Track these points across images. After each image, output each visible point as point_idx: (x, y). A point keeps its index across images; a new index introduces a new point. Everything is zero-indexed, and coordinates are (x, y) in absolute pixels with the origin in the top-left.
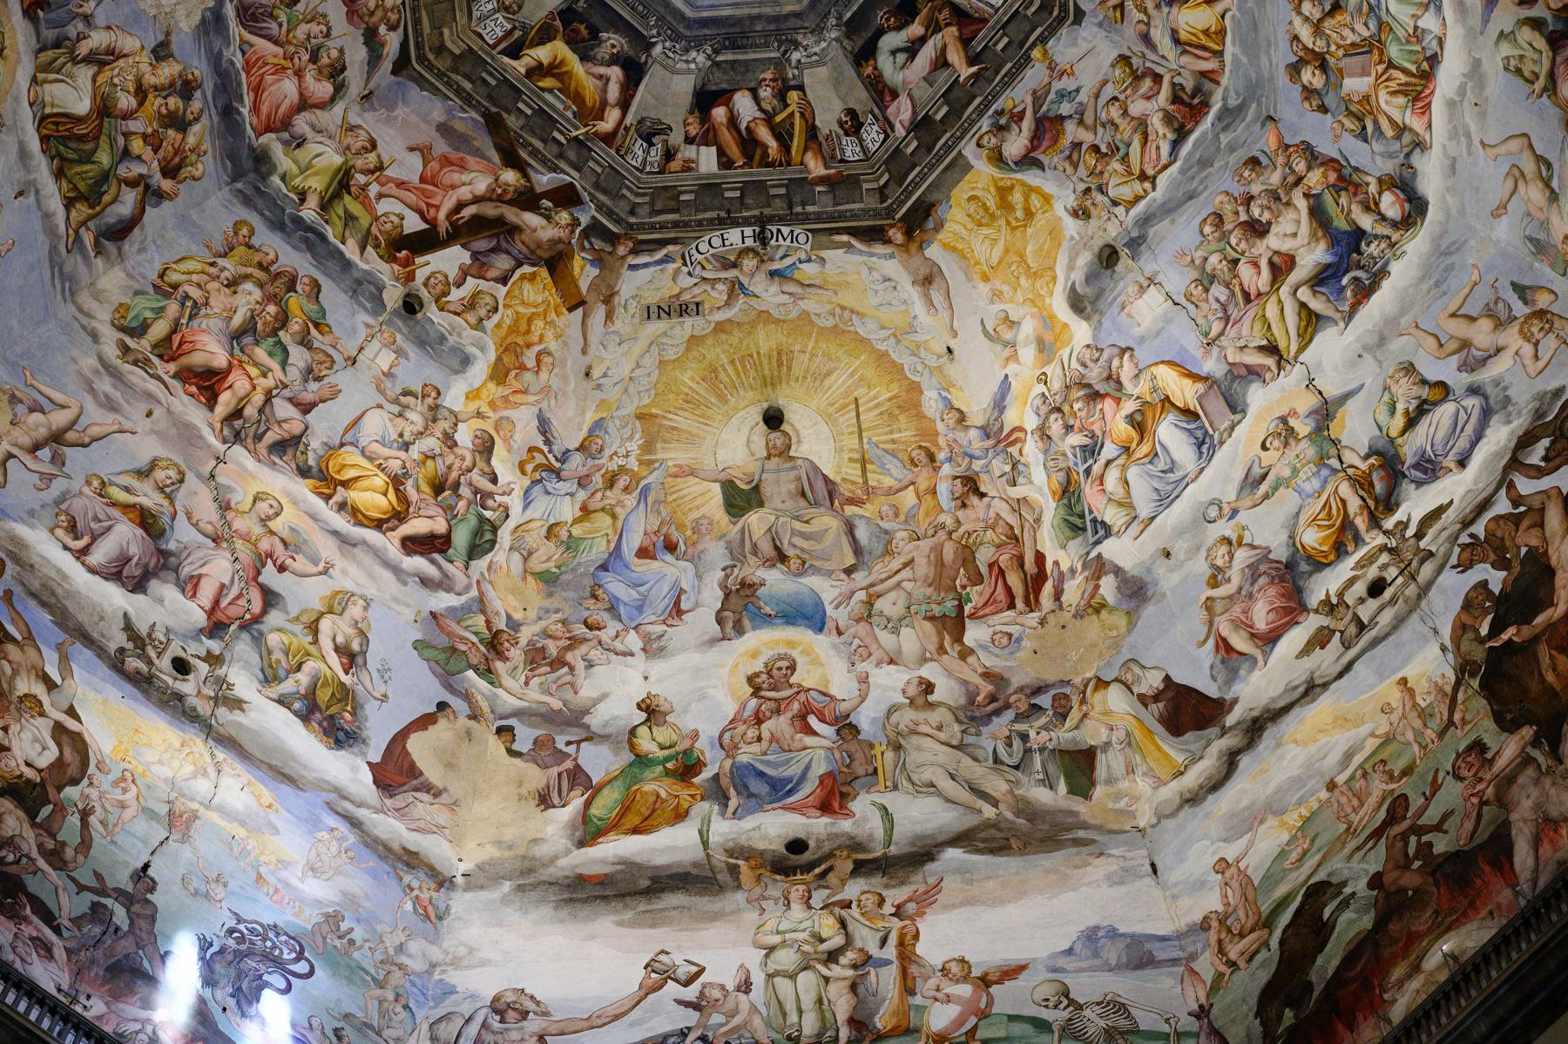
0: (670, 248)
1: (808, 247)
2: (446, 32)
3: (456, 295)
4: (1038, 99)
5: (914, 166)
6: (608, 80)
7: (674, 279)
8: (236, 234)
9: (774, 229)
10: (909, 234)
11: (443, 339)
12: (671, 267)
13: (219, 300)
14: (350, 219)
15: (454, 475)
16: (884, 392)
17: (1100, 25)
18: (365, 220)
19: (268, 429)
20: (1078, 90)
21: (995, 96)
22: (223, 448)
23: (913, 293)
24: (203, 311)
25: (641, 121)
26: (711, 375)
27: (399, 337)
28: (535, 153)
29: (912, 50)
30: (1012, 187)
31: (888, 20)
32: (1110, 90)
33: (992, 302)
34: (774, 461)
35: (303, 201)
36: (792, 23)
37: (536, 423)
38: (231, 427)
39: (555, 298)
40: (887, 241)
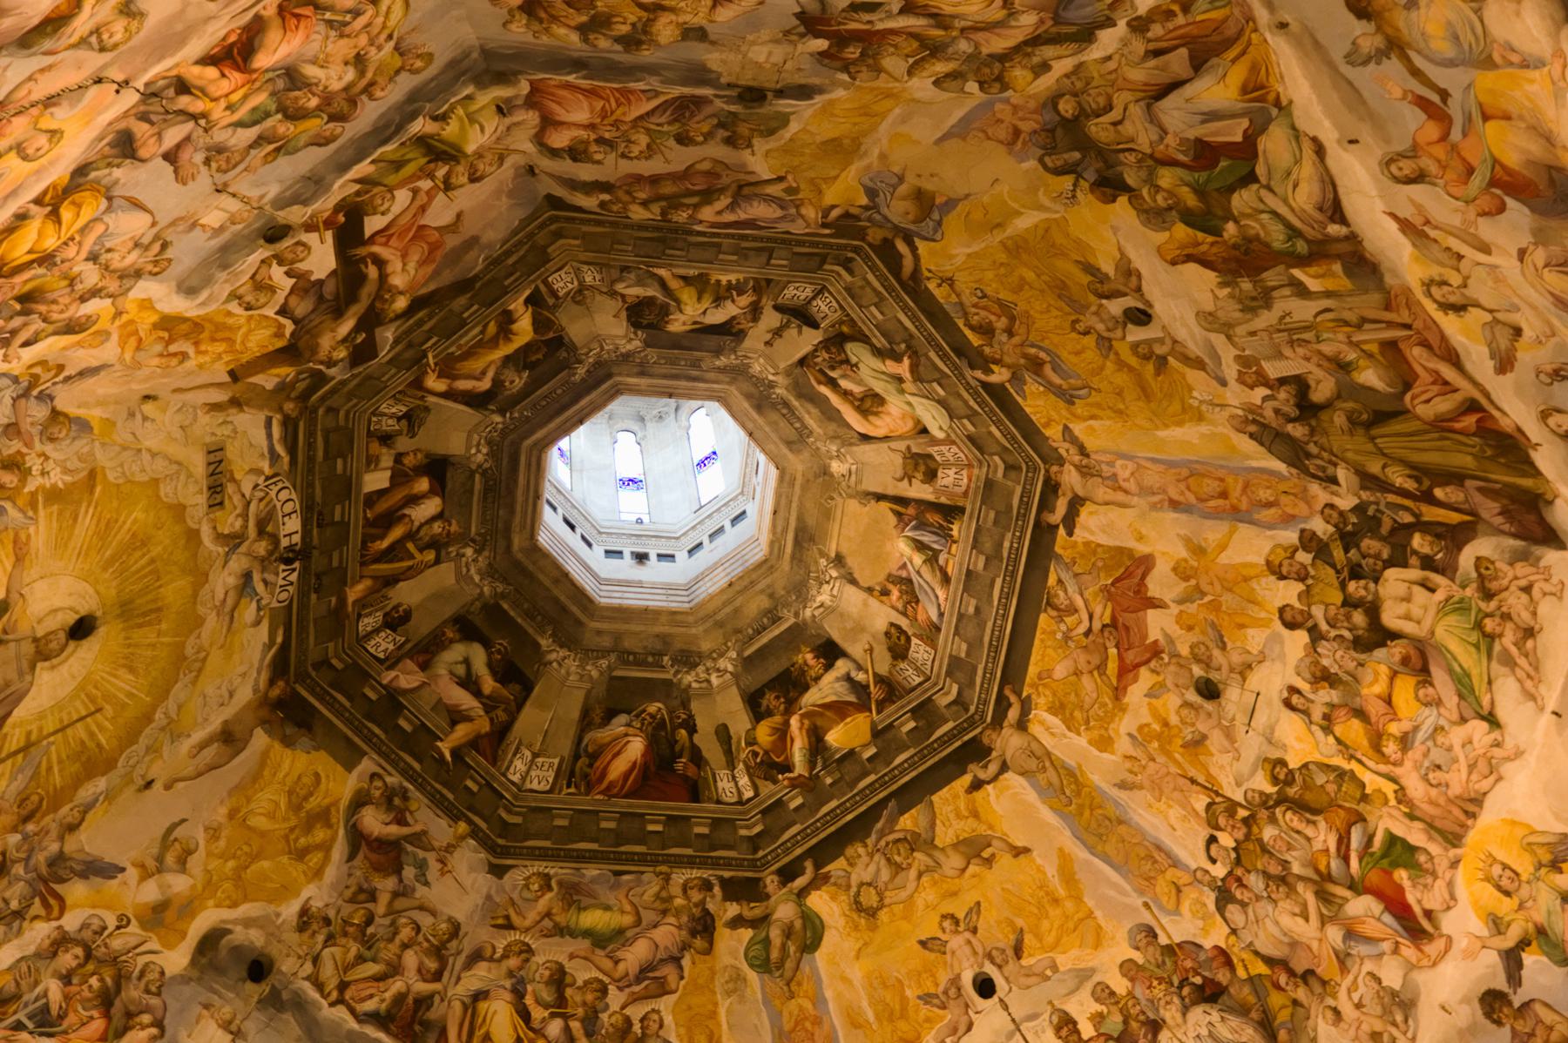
0: (286, 459)
1: (275, 604)
2: (577, 242)
3: (277, 273)
4: (419, 839)
5: (350, 698)
6: (478, 379)
7: (252, 471)
8: (418, 56)
9: (297, 565)
10: (279, 704)
11: (224, 267)
12: (265, 466)
13: (342, 48)
14: (398, 165)
15: (42, 308)
16: (105, 732)
17: (489, 897)
18: (391, 179)
19: (152, 123)
20: (426, 884)
21: (421, 787)
22: (140, 84)
23: (215, 724)
24: (333, 33)
25: (427, 409)
26: (139, 542)
27: (239, 227)
28: (420, 323)
29: (469, 683)
30: (329, 825)
31: (499, 652)
32: (426, 920)
33: (206, 829)
34: (28, 648)
35: (435, 118)
36: (502, 544)
37: (95, 363)
38: (167, 87)
39: (245, 358)
40: (272, 682)
